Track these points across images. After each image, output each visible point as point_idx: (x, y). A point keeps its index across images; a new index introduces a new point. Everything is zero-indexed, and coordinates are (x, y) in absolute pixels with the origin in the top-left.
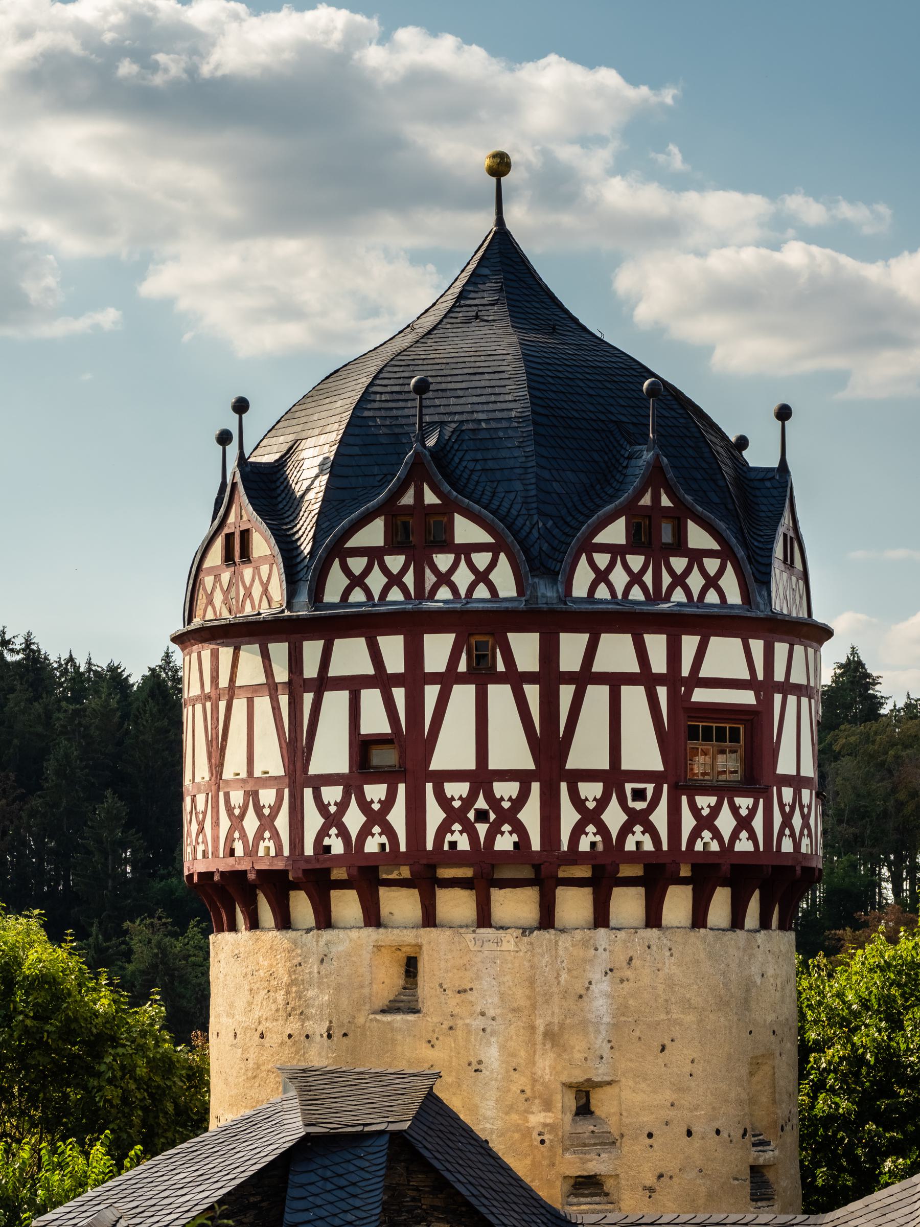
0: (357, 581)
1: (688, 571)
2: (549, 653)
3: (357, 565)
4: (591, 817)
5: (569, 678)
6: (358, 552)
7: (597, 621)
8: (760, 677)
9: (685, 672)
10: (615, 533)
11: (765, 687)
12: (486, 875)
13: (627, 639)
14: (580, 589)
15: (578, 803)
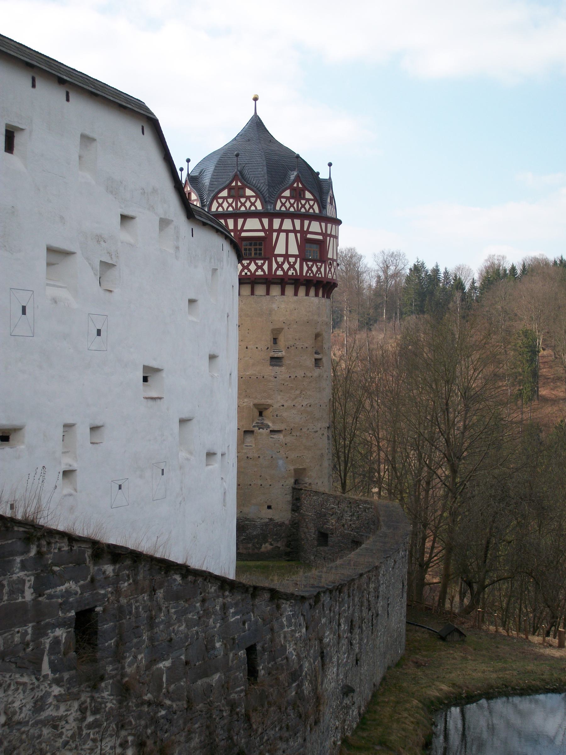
0: (220, 205)
1: (305, 204)
2: (271, 224)
3: (220, 201)
4: (280, 266)
5: (275, 231)
6: (221, 198)
7: (283, 215)
8: (324, 232)
9: (305, 229)
10: (287, 193)
11: (325, 235)
13: (290, 220)
14: (278, 208)
15: (277, 262)
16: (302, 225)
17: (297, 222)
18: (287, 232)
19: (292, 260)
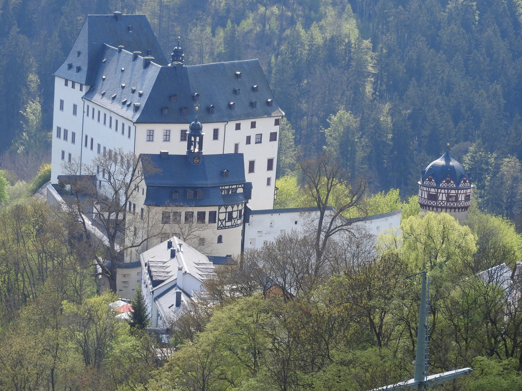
4: (440, 203)
7: (441, 189)
16: (448, 191)
17: (446, 191)
18: (443, 193)
19: (444, 202)
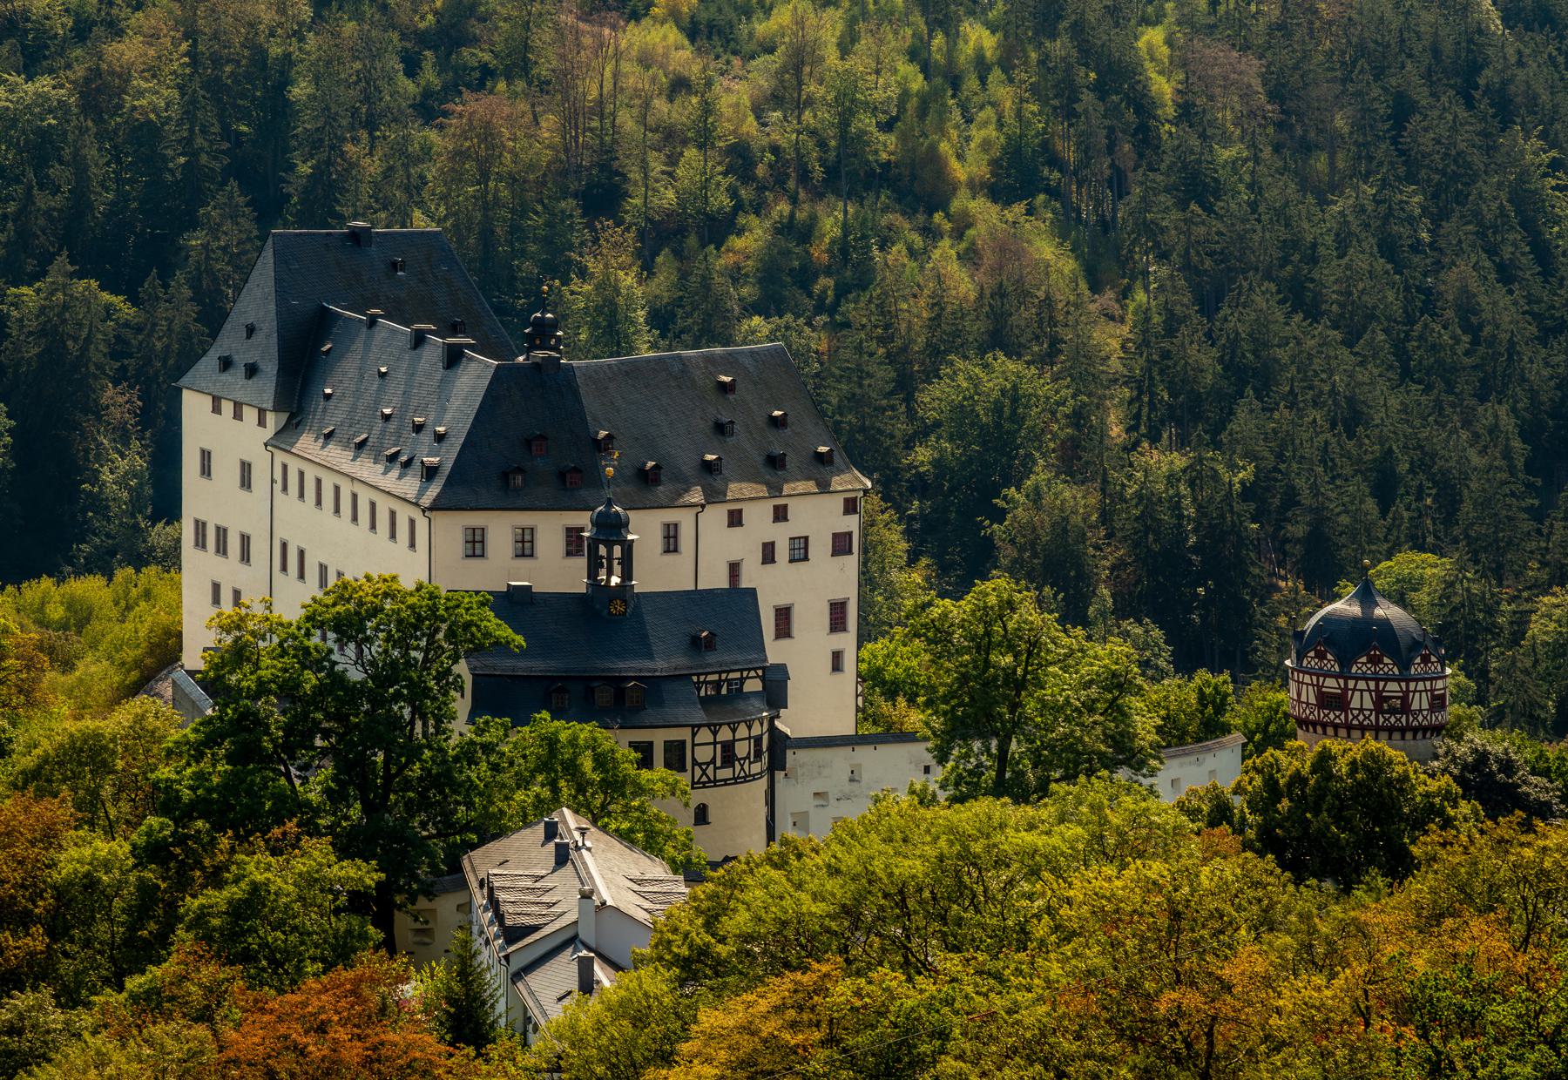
7: (1357, 679)
12: (1363, 729)
18: (1362, 691)
